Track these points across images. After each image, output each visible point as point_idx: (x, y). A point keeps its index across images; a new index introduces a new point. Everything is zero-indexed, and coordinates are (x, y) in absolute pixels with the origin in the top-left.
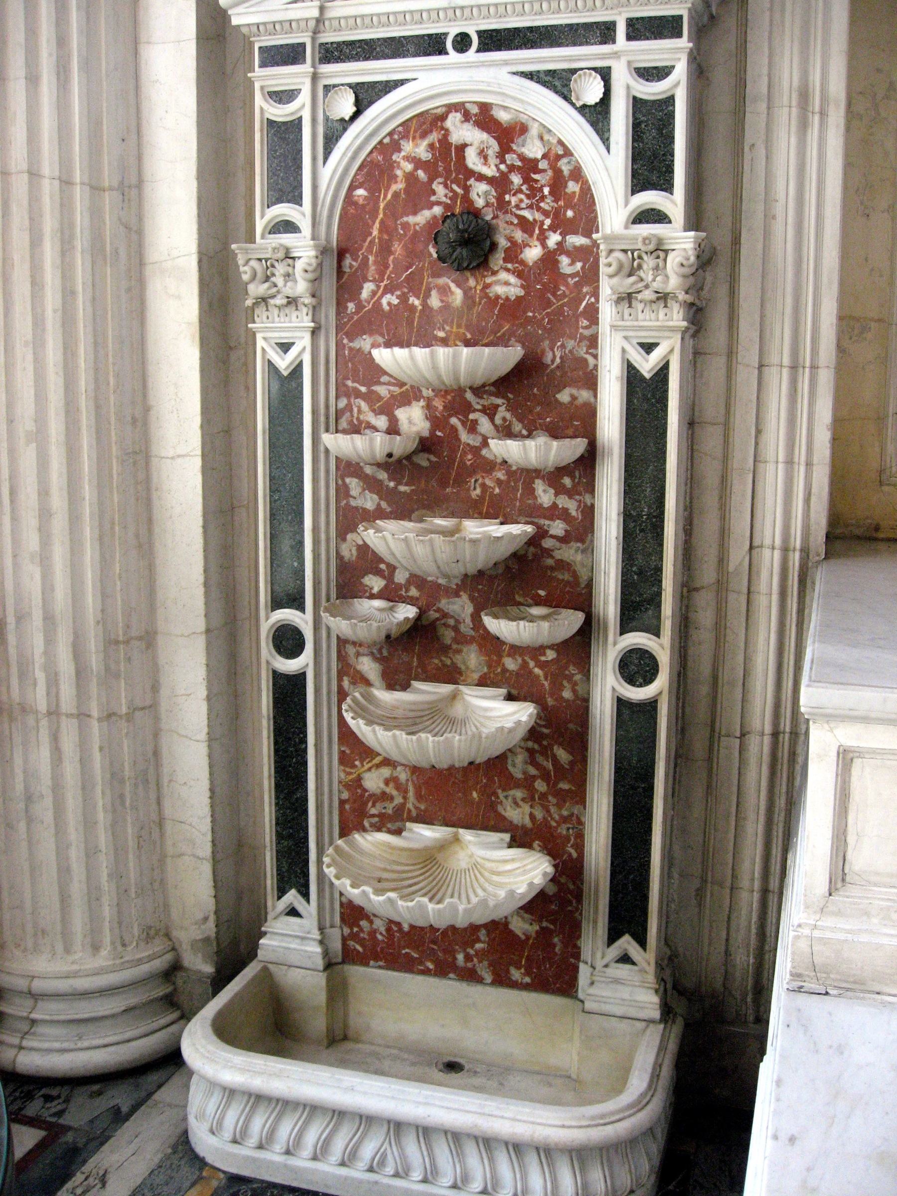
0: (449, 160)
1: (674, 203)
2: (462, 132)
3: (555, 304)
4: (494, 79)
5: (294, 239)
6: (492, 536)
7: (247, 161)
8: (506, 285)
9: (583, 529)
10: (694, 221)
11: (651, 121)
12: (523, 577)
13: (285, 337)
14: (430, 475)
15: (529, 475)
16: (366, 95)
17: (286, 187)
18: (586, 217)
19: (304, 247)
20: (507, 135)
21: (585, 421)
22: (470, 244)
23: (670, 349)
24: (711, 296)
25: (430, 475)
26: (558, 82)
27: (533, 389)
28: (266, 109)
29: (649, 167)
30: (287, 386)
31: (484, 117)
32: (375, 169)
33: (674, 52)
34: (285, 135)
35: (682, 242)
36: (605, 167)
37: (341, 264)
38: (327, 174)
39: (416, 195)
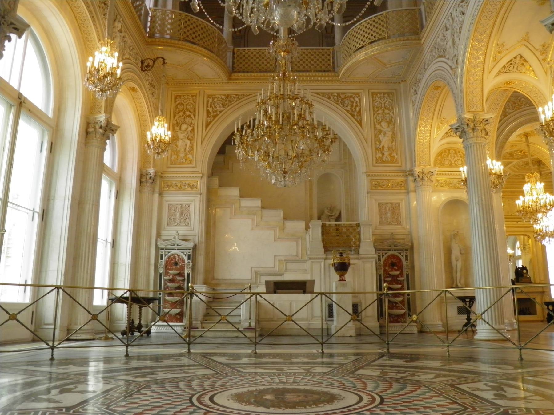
0: (174, 258)
1: (191, 261)
2: (176, 256)
3: (182, 268)
4: (178, 252)
5: (163, 263)
6: (177, 285)
7: (158, 257)
8: (178, 267)
9: (184, 284)
10: (192, 262)
11: (189, 256)
12: (179, 288)
13: (161, 270)
14: (172, 281)
15: (180, 280)
16: (168, 253)
17: (162, 259)
18: (184, 262)
19: (163, 263)
20: (179, 256)
21: (184, 276)
22: (176, 264)
23: (190, 271)
24: (193, 268)
25: (172, 281)
26: (183, 253)
27: (181, 274)
28: (160, 253)
29: (189, 259)
30: (161, 275)
31: (177, 255)
32: (169, 258)
33: (191, 251)
34: (162, 255)
35: (191, 264)
36: (186, 258)
37: (166, 266)
38: (165, 258)
39: (172, 260)
